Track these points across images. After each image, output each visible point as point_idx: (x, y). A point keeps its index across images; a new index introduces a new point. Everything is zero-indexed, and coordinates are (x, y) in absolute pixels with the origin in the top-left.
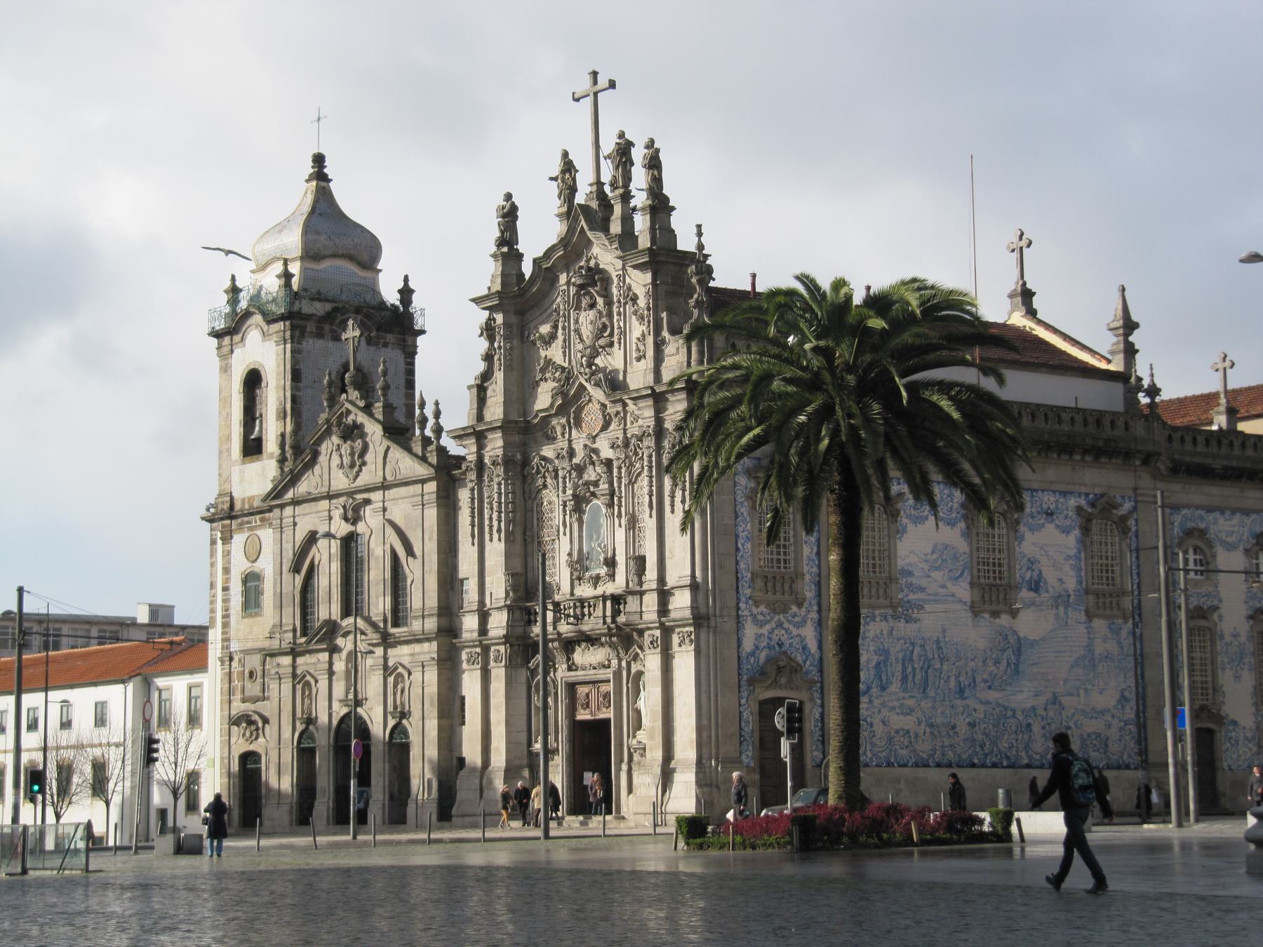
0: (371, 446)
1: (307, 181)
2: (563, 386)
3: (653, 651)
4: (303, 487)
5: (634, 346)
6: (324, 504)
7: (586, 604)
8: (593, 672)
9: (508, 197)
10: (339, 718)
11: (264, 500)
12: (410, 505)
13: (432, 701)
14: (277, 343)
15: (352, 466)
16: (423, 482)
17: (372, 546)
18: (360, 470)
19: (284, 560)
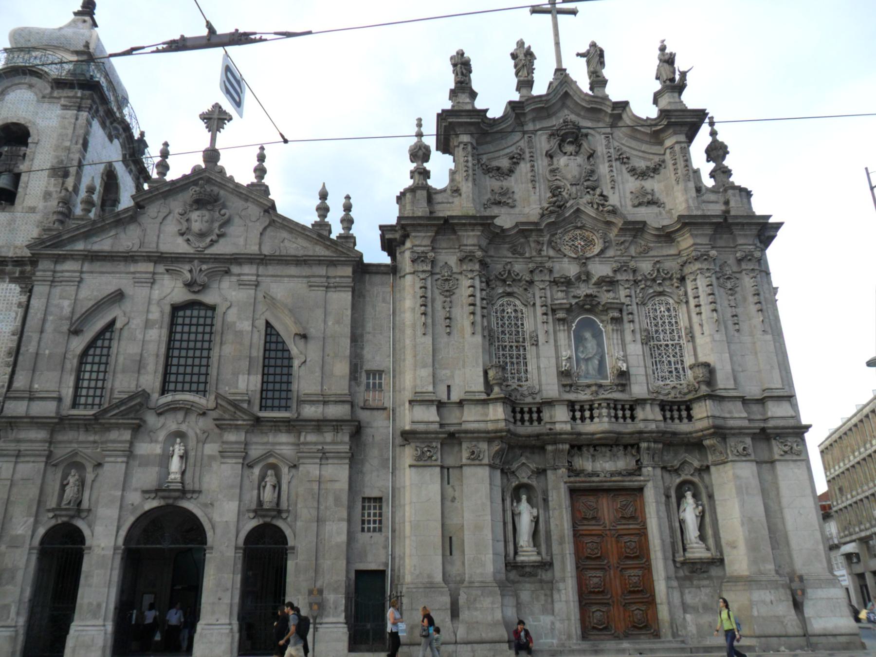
0: (236, 220)
1: (76, 14)
2: (560, 207)
3: (744, 459)
4: (103, 244)
5: (628, 195)
6: (150, 267)
7: (619, 407)
8: (620, 478)
9: (461, 54)
10: (139, 513)
11: (28, 247)
12: (305, 286)
13: (337, 500)
14: (65, 107)
15: (202, 235)
16: (332, 263)
17: (232, 316)
18: (216, 241)
19: (50, 318)
